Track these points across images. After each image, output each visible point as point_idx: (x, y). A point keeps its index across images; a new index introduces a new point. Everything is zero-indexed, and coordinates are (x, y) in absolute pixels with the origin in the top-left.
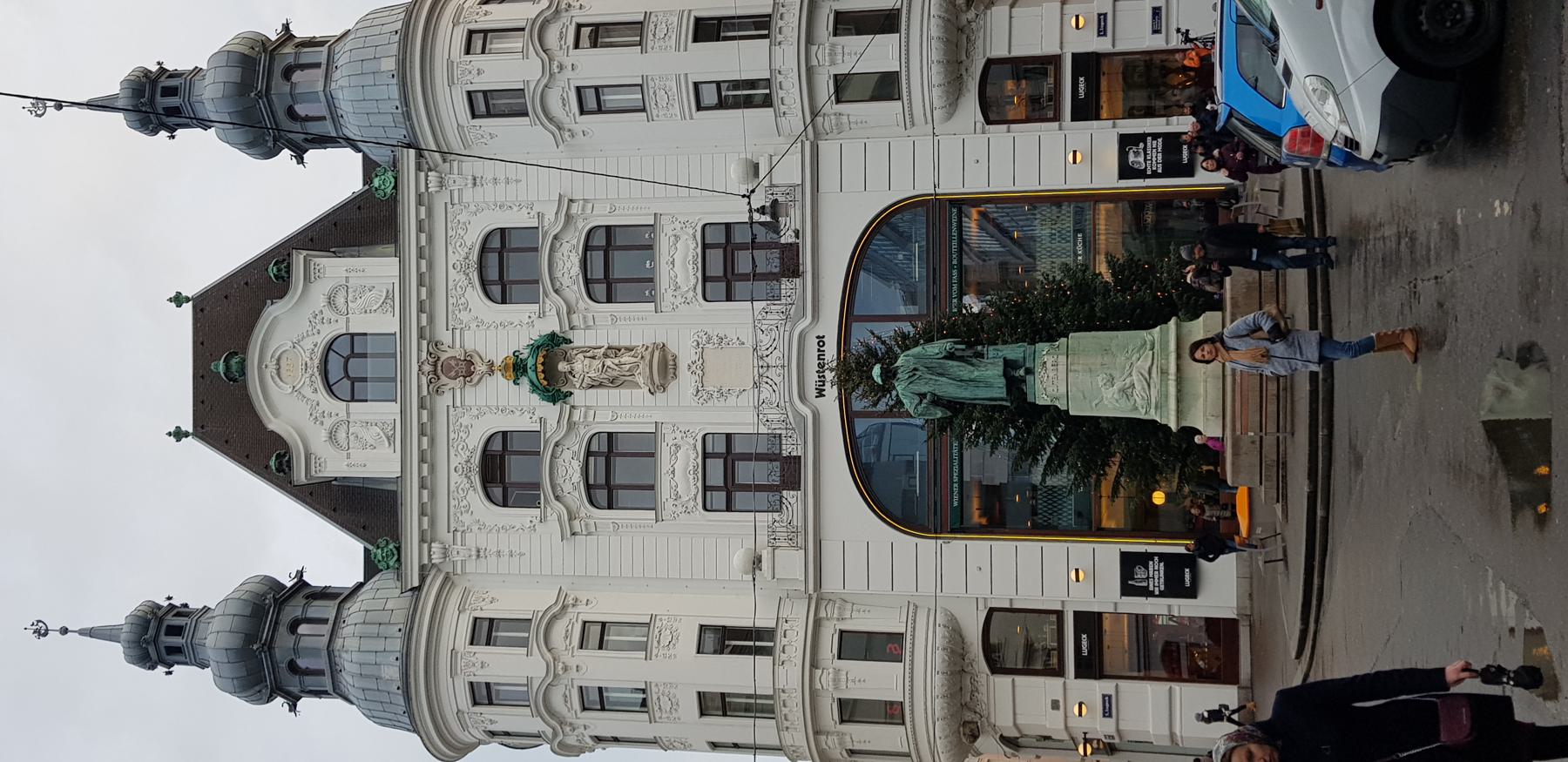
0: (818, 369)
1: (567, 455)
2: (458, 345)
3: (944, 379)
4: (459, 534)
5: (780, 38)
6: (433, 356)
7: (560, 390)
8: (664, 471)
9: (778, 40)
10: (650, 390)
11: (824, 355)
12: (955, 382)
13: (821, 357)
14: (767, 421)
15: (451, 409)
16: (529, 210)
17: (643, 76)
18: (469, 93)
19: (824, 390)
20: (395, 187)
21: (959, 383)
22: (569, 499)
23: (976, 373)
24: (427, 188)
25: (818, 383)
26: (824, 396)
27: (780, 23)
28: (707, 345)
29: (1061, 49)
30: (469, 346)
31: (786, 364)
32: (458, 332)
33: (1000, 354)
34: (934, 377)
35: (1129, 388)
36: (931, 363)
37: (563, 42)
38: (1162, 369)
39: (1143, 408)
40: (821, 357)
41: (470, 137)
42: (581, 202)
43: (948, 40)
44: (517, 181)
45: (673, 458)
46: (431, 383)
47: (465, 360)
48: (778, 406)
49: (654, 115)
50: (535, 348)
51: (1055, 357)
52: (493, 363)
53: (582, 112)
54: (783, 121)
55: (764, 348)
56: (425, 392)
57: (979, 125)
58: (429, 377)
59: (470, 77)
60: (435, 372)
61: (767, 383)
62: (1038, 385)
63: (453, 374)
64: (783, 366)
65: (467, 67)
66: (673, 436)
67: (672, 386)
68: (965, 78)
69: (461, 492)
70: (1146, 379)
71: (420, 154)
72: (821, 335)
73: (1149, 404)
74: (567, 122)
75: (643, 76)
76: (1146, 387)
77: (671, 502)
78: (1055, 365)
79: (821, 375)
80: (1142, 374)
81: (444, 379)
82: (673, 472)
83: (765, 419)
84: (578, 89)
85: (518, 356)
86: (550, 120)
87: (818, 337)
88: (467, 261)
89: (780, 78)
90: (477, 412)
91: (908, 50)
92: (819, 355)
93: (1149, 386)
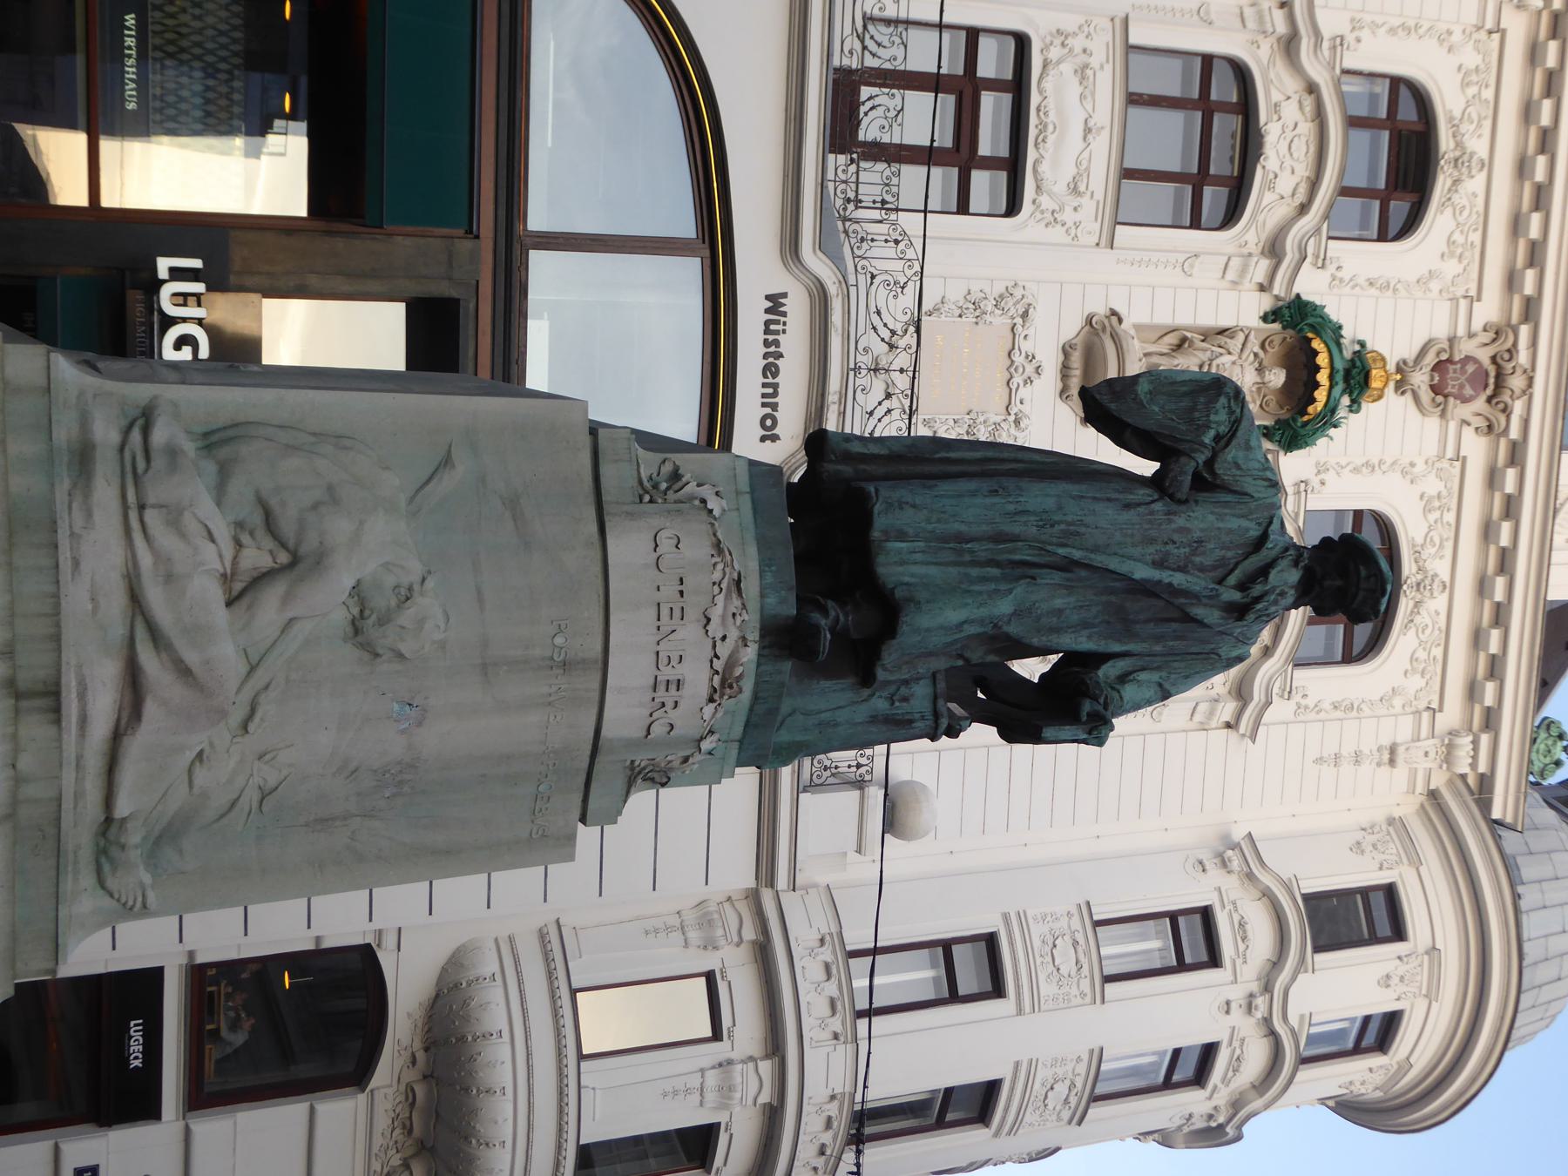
0: (780, 362)
1: (1286, 184)
2: (1452, 426)
3: (1142, 572)
4: (1489, 25)
5: (833, 1110)
6: (1501, 406)
7: (1284, 328)
8: (1105, 134)
9: (836, 1103)
10: (1120, 321)
11: (764, 396)
12: (1099, 560)
13: (770, 390)
15: (1473, 293)
16: (1303, 702)
17: (1103, 1001)
18: (1398, 933)
19: (767, 311)
20: (1534, 741)
21: (1077, 554)
22: (1292, 85)
23: (1004, 607)
24: (1476, 743)
25: (780, 327)
26: (768, 298)
27: (827, 1138)
28: (998, 419)
29: (187, 1132)
30: (1433, 423)
31: (851, 374)
32: (1450, 453)
33: (880, 704)
34: (1178, 579)
35: (261, 579)
36: (1159, 638)
37: (1238, 1052)
38: (56, 712)
39: (173, 453)
40: (770, 390)
41: (1393, 849)
42: (1214, 724)
43: (467, 1139)
44: (1320, 760)
45: (1085, 164)
46: (1509, 351)
47: (1446, 396)
48: (873, 277)
49: (1076, 919)
50: (1328, 419)
51: (658, 730)
53: (1206, 914)
54: (824, 925)
55: (896, 414)
56: (1524, 330)
57: (390, 941)
58: (1513, 364)
59: (1402, 969)
60: (1500, 376)
61: (891, 331)
62: (748, 562)
63: (1470, 368)
64: (857, 369)
65: (1405, 989)
66: (1078, 217)
67: (1072, 327)
68: (418, 1045)
69: (1475, 116)
70: (156, 637)
71: (1485, 804)
72: (768, 442)
73: (133, 474)
74: (1232, 885)
75: (1103, 1001)
76: (155, 596)
77: (1095, 61)
78: (665, 687)
79: (772, 349)
80: (184, 672)
81: (1484, 356)
82: (1087, 130)
83: (901, 246)
84: (1214, 960)
85: (1353, 401)
86: (1267, 894)
87: (774, 438)
88: (1419, 597)
89: (836, 1024)
91: (561, 1111)
92: (775, 394)
93: (136, 599)
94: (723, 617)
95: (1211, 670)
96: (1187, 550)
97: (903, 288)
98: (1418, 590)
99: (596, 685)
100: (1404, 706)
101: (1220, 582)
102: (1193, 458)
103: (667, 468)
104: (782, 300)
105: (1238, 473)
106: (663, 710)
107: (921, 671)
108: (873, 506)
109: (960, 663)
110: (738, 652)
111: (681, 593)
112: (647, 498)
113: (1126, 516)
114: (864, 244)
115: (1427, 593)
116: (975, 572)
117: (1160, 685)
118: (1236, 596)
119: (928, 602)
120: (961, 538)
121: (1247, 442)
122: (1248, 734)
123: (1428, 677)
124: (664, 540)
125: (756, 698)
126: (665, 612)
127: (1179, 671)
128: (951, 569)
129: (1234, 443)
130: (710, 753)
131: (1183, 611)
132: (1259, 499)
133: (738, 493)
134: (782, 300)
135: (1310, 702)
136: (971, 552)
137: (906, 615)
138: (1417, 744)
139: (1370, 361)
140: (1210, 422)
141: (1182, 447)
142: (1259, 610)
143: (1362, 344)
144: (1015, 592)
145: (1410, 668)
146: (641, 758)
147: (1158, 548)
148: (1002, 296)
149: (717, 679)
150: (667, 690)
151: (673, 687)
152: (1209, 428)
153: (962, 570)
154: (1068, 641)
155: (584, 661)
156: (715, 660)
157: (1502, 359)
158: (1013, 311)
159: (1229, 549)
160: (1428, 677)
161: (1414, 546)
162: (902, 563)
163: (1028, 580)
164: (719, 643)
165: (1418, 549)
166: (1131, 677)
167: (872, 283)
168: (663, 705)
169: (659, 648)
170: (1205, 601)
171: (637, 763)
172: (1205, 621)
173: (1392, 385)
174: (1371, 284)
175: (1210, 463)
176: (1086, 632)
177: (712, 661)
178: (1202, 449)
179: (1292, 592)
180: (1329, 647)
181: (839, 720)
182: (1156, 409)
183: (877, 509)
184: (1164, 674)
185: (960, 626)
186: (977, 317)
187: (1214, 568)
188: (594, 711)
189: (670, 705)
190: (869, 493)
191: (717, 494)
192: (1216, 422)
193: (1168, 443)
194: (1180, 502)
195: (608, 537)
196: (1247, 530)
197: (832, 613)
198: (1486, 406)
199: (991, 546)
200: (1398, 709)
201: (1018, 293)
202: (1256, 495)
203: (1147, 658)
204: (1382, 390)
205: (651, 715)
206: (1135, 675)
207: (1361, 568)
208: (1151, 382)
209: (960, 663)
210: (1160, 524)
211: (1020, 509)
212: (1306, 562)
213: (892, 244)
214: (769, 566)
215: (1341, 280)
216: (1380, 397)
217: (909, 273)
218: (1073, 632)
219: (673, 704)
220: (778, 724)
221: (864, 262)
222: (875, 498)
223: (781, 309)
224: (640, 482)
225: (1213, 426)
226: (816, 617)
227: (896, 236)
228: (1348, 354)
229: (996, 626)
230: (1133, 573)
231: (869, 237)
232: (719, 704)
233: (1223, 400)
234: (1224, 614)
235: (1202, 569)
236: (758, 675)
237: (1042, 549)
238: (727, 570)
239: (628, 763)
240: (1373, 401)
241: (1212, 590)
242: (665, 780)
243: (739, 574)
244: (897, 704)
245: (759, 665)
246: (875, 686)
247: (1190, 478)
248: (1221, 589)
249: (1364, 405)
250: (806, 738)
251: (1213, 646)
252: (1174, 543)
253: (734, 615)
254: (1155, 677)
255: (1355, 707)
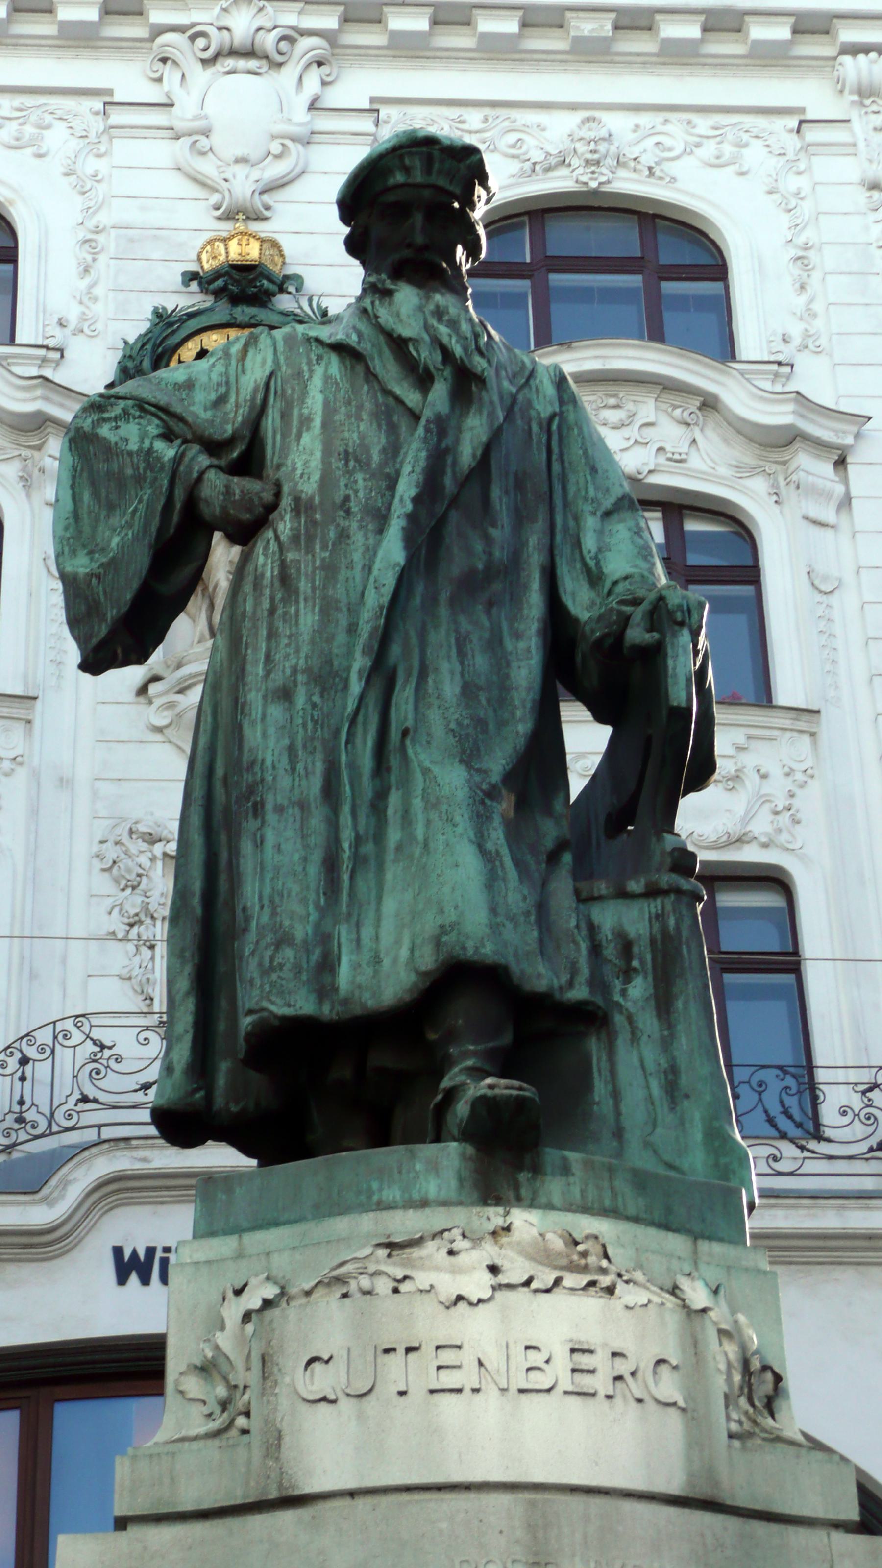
6: (284, 45)
14: (24, 1061)
16: (797, 341)
19: (145, 1280)
21: (360, 662)
24: (855, 50)
26: (122, 1280)
42: (840, 489)
48: (85, 1099)
52: (266, 219)
58: (212, 31)
83: (31, 1052)
88: (610, 162)
90: (90, 171)
94: (455, 1271)
95: (580, 429)
96: (359, 477)
97: (103, 1047)
98: (598, 163)
99: (577, 1502)
100: (799, 173)
101: (416, 417)
102: (202, 474)
103: (194, 1386)
104: (127, 1255)
105: (232, 399)
106: (628, 1377)
107: (573, 923)
108: (276, 1016)
109: (567, 858)
110: (519, 1243)
111: (409, 1350)
112: (241, 1421)
113: (304, 586)
114: (30, 1116)
115: (602, 147)
116: (394, 836)
117: (607, 514)
118: (440, 391)
119: (441, 911)
120: (331, 864)
121: (178, 387)
122: (855, 429)
123: (745, 137)
124: (314, 1388)
125: (611, 1212)
126: (448, 1379)
127: (582, 481)
128: (389, 876)
129: (178, 409)
130: (716, 1292)
131: (468, 478)
132: (276, 361)
133: (240, 1255)
134: (127, 1255)
135: (796, 330)
136: (358, 840)
137: (464, 948)
138: (861, 144)
139: (215, 263)
140: (140, 450)
141: (179, 495)
142: (465, 349)
143: (191, 277)
144: (427, 764)
145: (731, 168)
146: (723, 1419)
147: (355, 525)
148: (117, 881)
149: (571, 1280)
150: (592, 1372)
151: (585, 1361)
152: (150, 451)
153: (390, 856)
154: (524, 672)
155: (531, 1528)
156: (534, 1285)
157: (206, 49)
158: (144, 860)
159: (360, 407)
160: (745, 137)
161: (522, 174)
162: (377, 960)
163: (408, 742)
164: (502, 1279)
165: (527, 166)
166: (592, 563)
167: (96, 1101)
168: (619, 1378)
169: (513, 1388)
170: (447, 442)
171: (734, 1427)
172: (484, 439)
173: (255, 227)
174: (86, 270)
175: (213, 447)
176: (509, 644)
177: (536, 1291)
178: (186, 459)
179: (438, 298)
180: (702, 303)
181: (664, 1064)
182: (116, 540)
183: (280, 1009)
184: (588, 508)
185: (488, 857)
186: (152, 917)
187: (392, 429)
188: (628, 1506)
189: (623, 1367)
190: (254, 1024)
191: (238, 1292)
192: (142, 441)
193: (176, 518)
194: (278, 495)
195: (307, 1490)
196: (327, 378)
197: (462, 1078)
198: (284, 70)
199: (346, 809)
200: (803, 183)
201: (112, 852)
202: (268, 368)
203: (558, 538)
204: (263, 241)
205: (640, 1401)
206: (588, 559)
207: (391, 181)
208: (74, 552)
209: (567, 858)
210: (315, 523)
211: (284, 762)
212: (384, 276)
213: (28, 1068)
214: (370, 1193)
215: (83, 318)
216: (275, 244)
217: (77, 1037)
218: (508, 665)
219: (618, 1360)
220: (673, 1174)
221: (59, 1116)
222: (265, 1014)
223: (142, 1254)
224: (216, 1434)
225: (147, 444)
226: (462, 1109)
227: (13, 1063)
228: (208, 301)
229: (492, 793)
230: (398, 564)
231: (16, 1108)
232: (620, 1275)
233: (105, 431)
234: (473, 411)
235: (393, 450)
236: (570, 1208)
237: (353, 722)
238: (372, 1268)
239: (736, 1443)
240: (282, 256)
241: (427, 430)
242: (769, 1376)
243: (379, 1245)
244: (635, 963)
245: (549, 1207)
246: (599, 1000)
247: (236, 479)
248: (427, 414)
249: (290, 271)
250: (697, 1116)
251: (535, 428)
252: (347, 499)
253: (451, 1253)
254: (591, 523)
255: (801, 253)
